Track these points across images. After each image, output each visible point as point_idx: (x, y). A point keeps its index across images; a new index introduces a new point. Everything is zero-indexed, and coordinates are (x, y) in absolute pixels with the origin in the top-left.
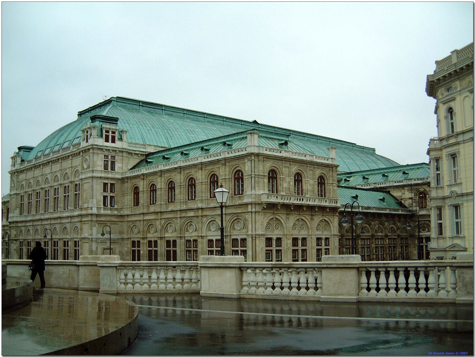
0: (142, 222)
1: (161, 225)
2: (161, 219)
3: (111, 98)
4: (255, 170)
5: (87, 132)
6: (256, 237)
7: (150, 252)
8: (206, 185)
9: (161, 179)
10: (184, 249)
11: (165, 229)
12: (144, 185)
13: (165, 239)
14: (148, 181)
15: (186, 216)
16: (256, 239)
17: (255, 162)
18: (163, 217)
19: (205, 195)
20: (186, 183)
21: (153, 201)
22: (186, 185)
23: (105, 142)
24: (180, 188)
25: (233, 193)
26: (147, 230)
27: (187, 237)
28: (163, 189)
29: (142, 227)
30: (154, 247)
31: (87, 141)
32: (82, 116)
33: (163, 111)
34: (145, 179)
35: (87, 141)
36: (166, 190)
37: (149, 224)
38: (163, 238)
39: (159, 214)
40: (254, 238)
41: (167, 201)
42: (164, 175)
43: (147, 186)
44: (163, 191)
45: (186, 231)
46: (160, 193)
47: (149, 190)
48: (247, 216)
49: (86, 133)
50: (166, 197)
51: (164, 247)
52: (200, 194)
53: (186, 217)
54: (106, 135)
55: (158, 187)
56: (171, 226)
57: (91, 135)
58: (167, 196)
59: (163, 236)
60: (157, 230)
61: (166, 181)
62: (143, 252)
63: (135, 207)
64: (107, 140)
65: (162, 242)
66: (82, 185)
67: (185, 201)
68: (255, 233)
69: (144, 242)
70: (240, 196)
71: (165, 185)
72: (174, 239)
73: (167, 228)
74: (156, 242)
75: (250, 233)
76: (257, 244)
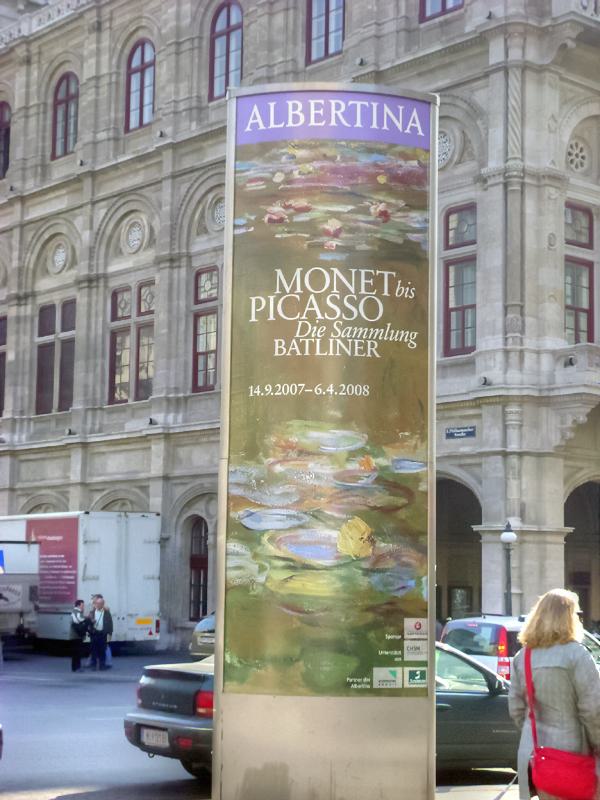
0: (16, 232)
1: (91, 228)
2: (94, 203)
6: (523, 185)
7: (45, 351)
8: (291, 12)
9: (98, 41)
10: (187, 307)
11: (107, 242)
12: (28, 86)
13: (106, 287)
14: (45, 66)
15: (197, 164)
16: (522, 192)
18: (101, 194)
19: (285, 55)
20: (201, 31)
21: (61, 141)
22: (200, 38)
24: (178, 53)
25: (415, 14)
26: (36, 265)
27: (199, 254)
28: (105, 81)
29: (16, 254)
34: (35, 59)
36: (117, 83)
37: (46, 236)
38: (98, 278)
39: (87, 183)
40: (513, 184)
41: (122, 127)
42: (111, 19)
43: (39, 87)
44: (104, 90)
45: (198, 234)
46: (93, 97)
47: (50, 101)
48: (480, 97)
50: (116, 111)
51: (101, 319)
52: (263, 53)
53: (197, 169)
55: (87, 72)
56: (133, 225)
58: (122, 105)
59: (101, 271)
60: (78, 253)
61: (119, 47)
62: (17, 355)
65: (94, 298)
67: (194, 104)
68: (518, 162)
69: (22, 314)
70: (448, 16)
71: (114, 61)
72: (142, 276)
73: (119, 240)
74: (69, 306)
75: (494, 163)
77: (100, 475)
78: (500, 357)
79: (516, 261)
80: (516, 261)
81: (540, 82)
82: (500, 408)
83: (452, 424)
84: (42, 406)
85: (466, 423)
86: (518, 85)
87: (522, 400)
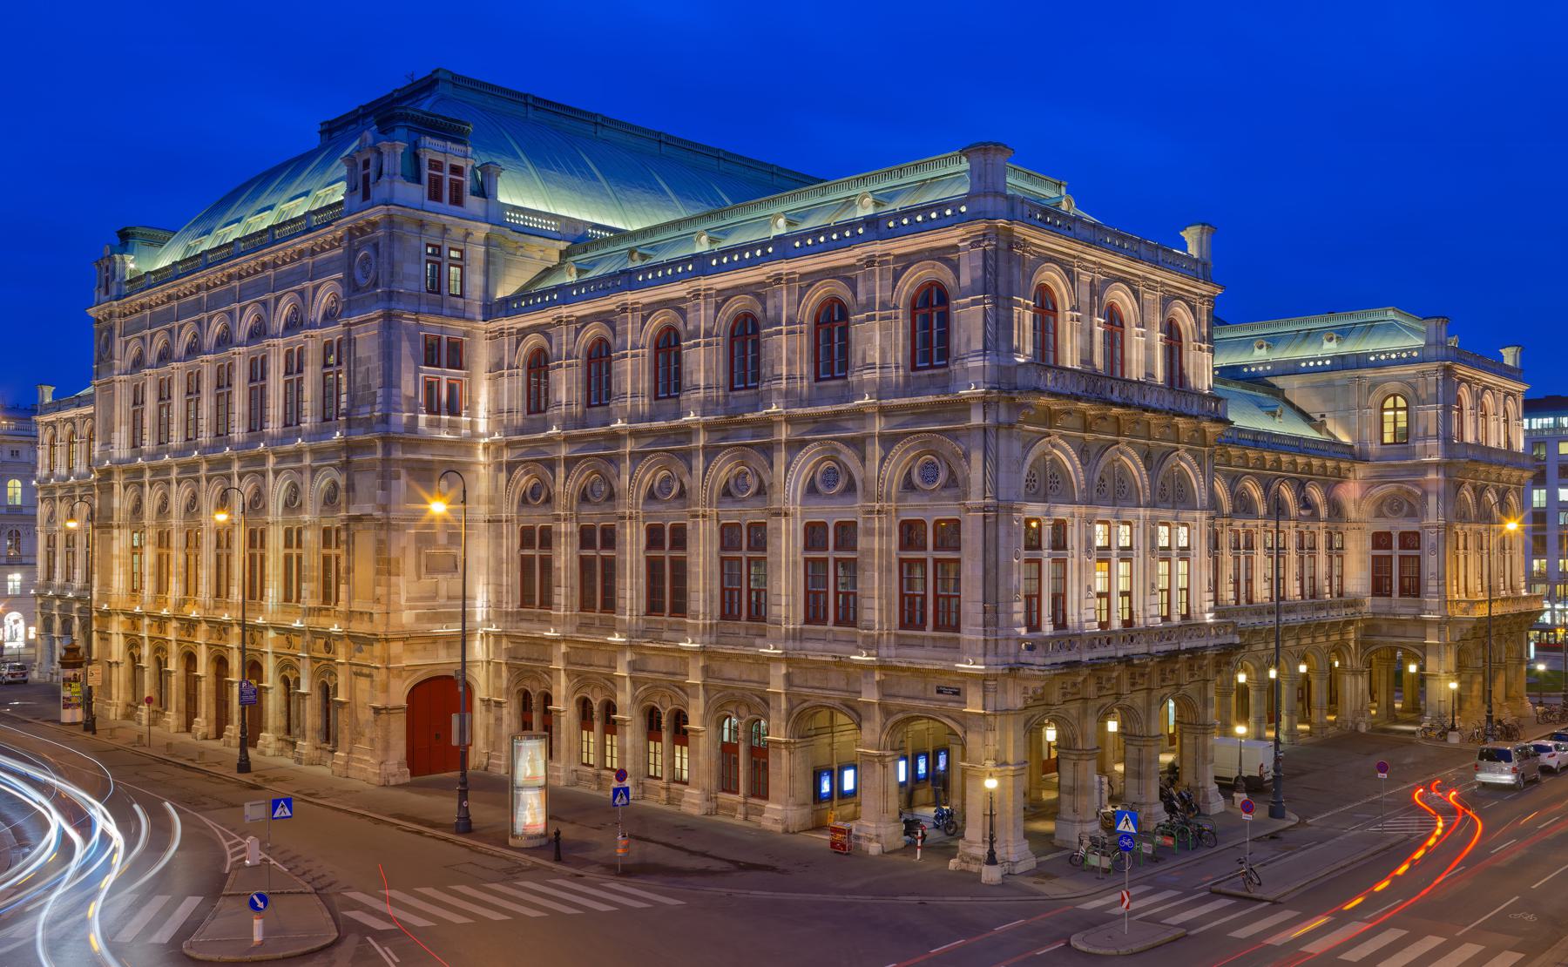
3: (437, 71)
4: (996, 280)
5: (366, 164)
17: (1000, 252)
23: (430, 198)
30: (603, 547)
31: (366, 196)
32: (335, 135)
33: (599, 128)
35: (366, 196)
49: (360, 166)
54: (430, 174)
57: (380, 174)
63: (533, 416)
64: (435, 195)
66: (350, 340)
70: (935, 371)
76: (1002, 541)
77: (644, 671)
78: (981, 645)
79: (993, 574)
80: (993, 574)
81: (1010, 436)
82: (981, 682)
83: (942, 683)
84: (586, 604)
85: (952, 685)
86: (994, 441)
87: (996, 677)
